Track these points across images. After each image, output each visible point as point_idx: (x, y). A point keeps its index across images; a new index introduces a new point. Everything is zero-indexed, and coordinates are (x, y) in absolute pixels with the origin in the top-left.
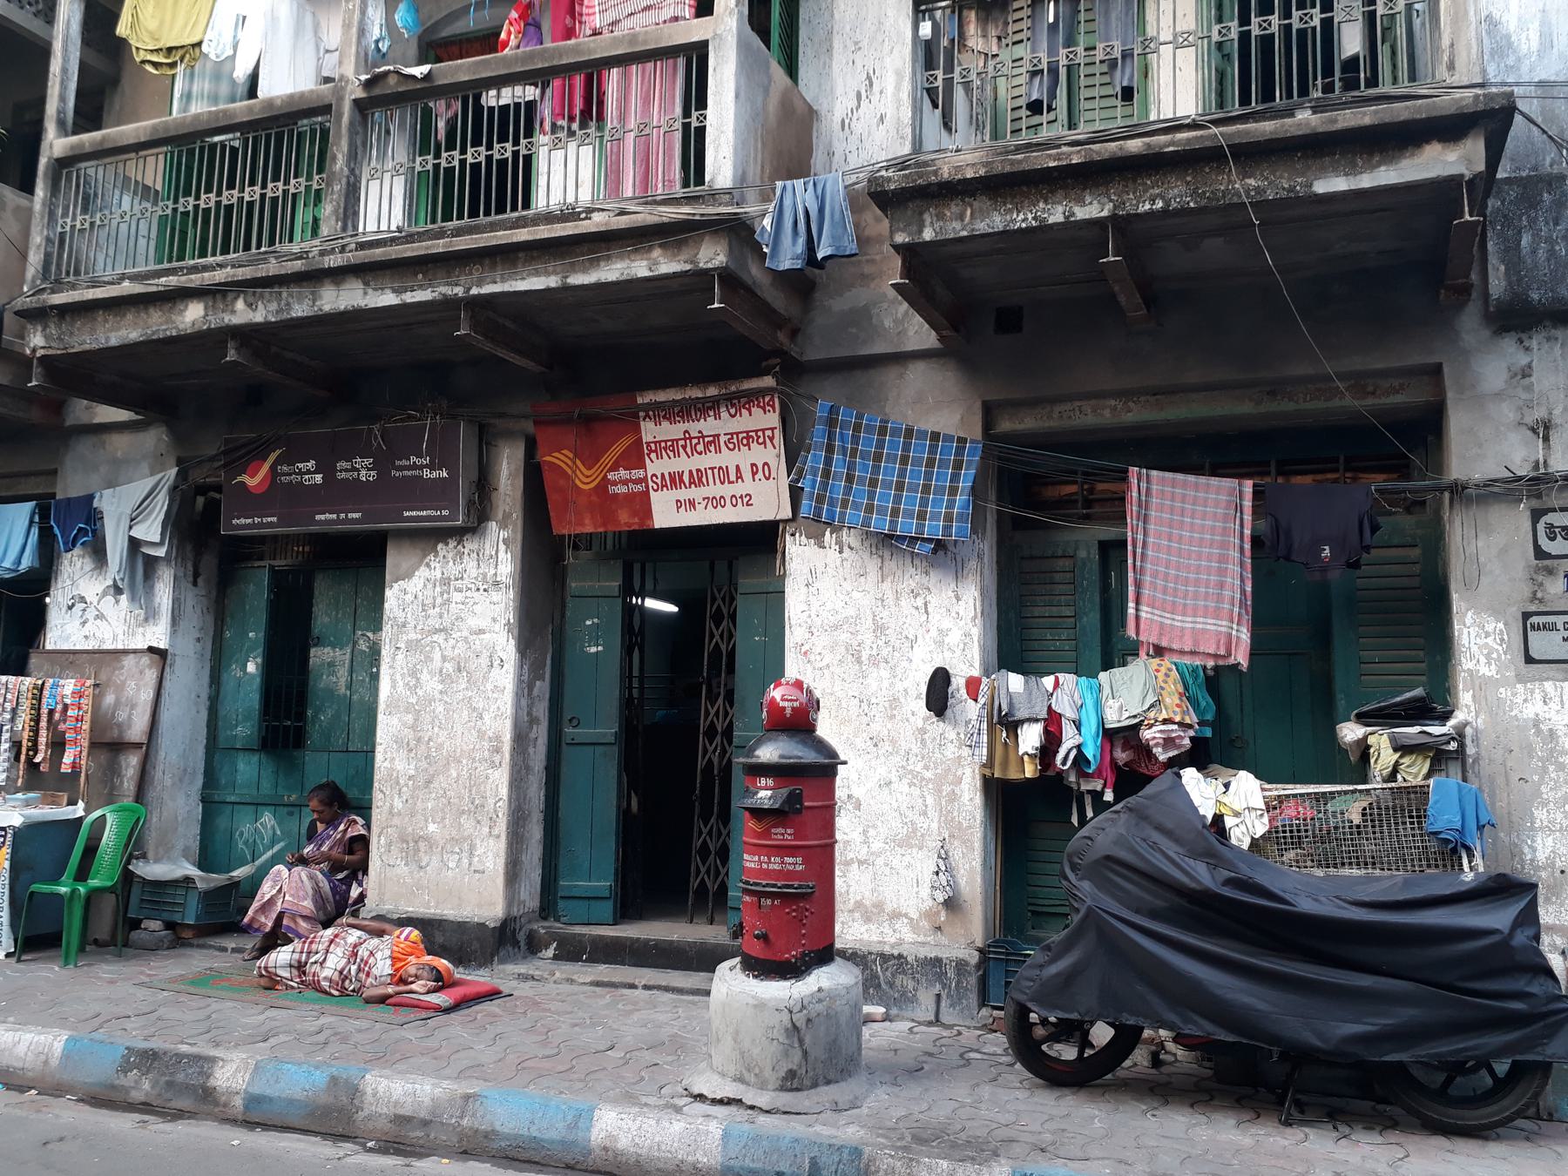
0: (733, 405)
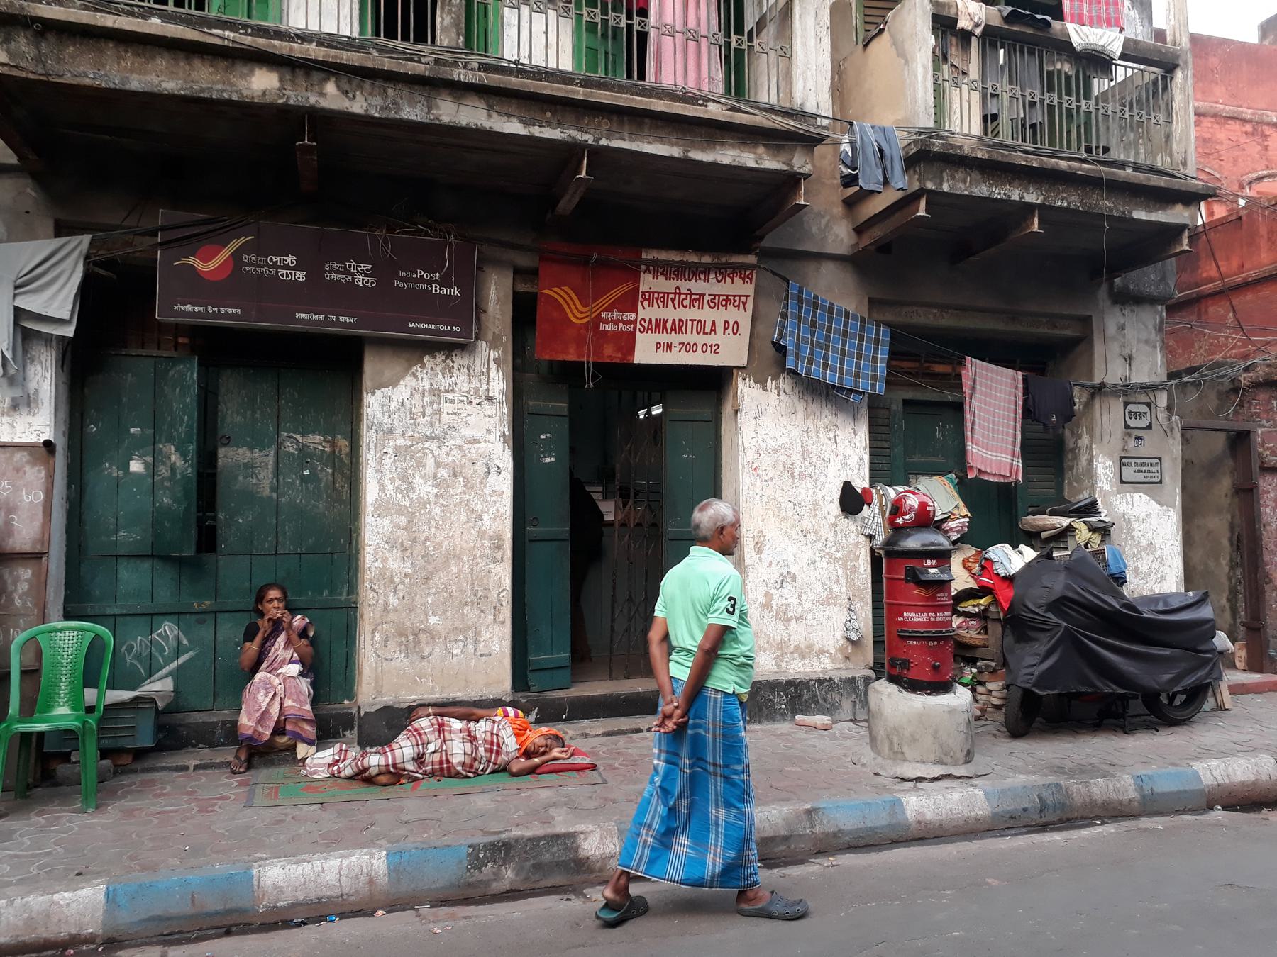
0: (721, 273)
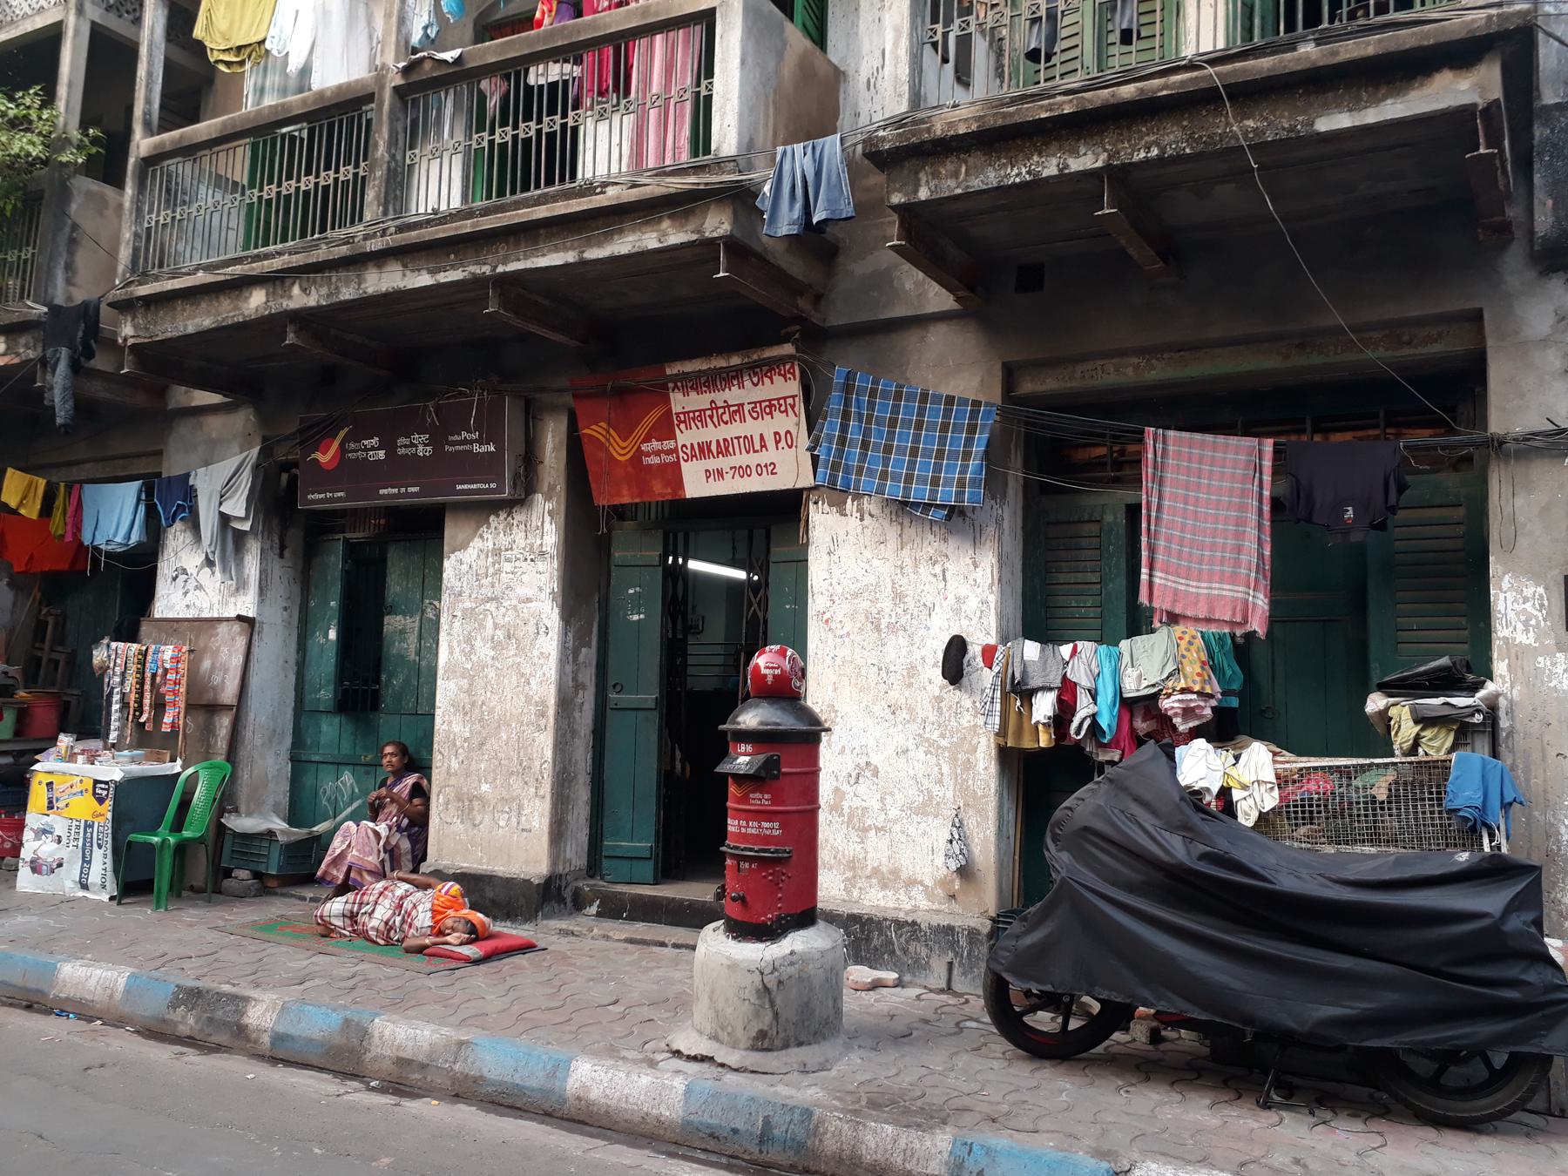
0: (755, 374)
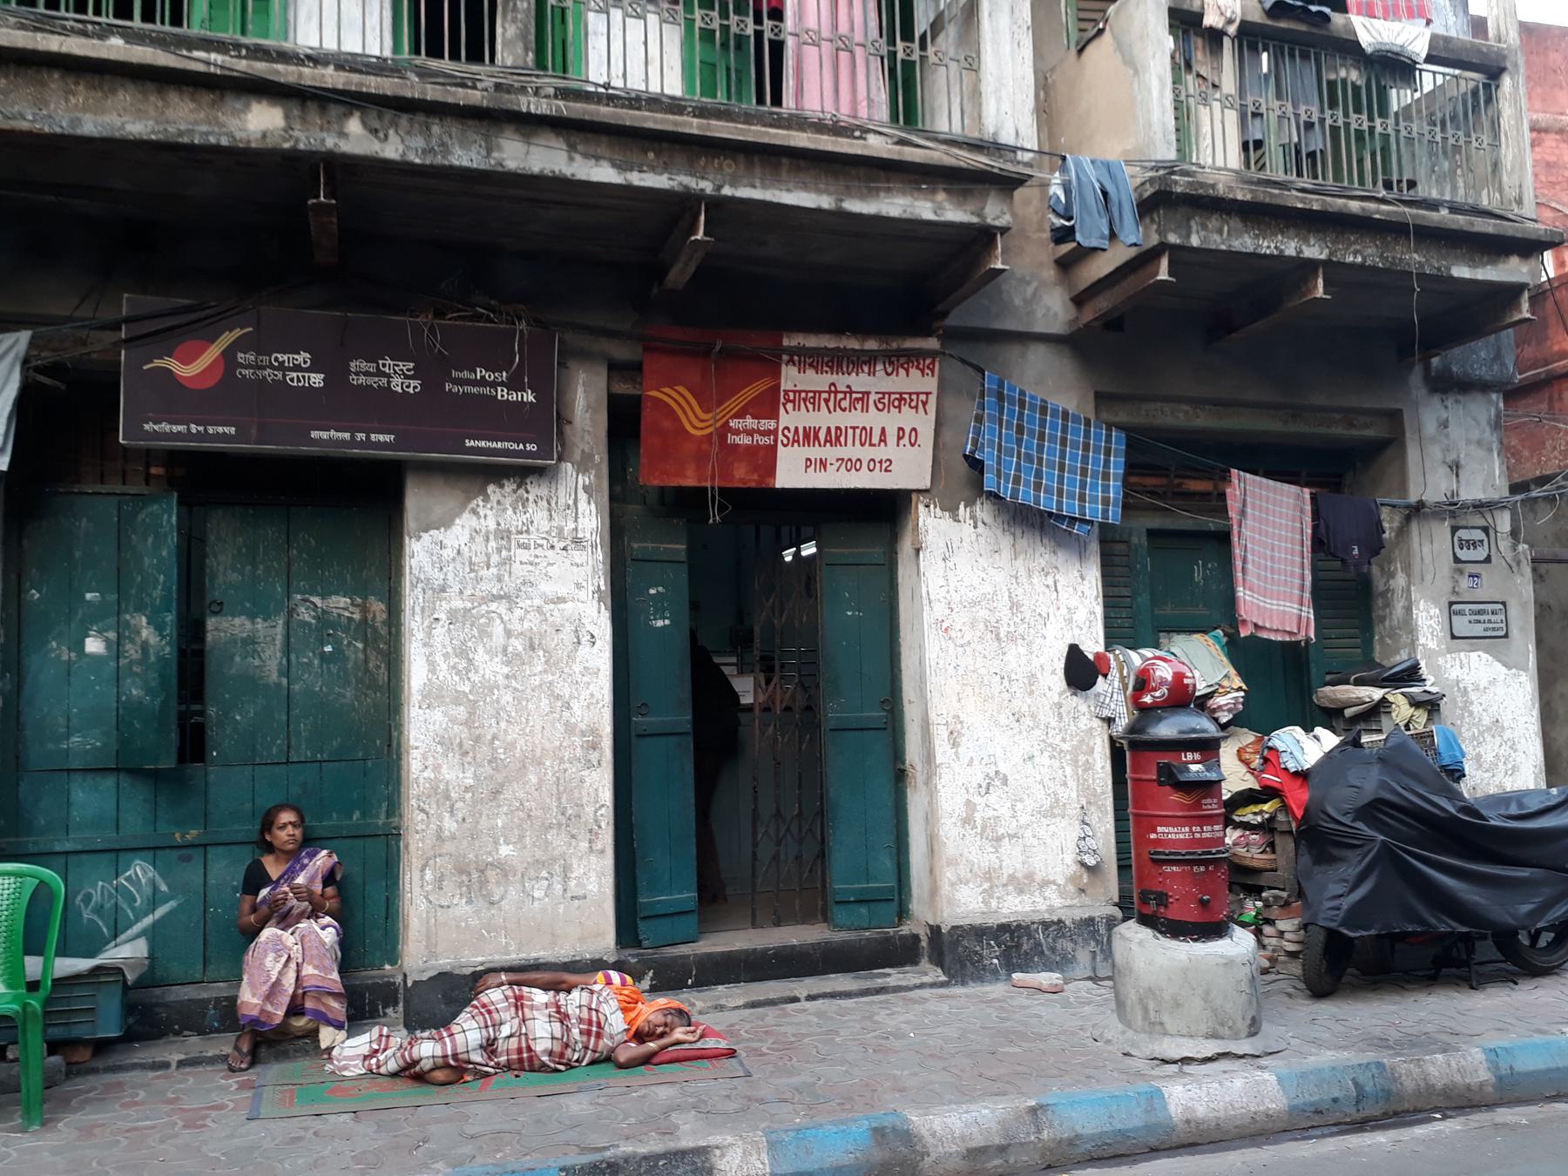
0: (891, 363)
